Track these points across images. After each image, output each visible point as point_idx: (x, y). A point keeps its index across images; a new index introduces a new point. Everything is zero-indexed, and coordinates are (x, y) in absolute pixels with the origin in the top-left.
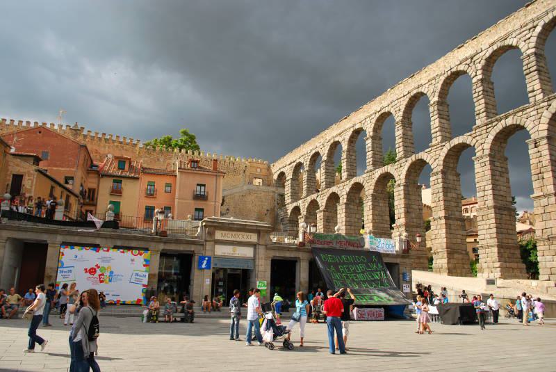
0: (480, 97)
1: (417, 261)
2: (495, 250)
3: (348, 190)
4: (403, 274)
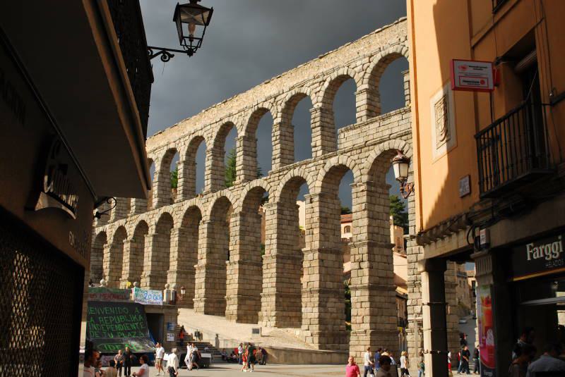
0: (277, 142)
1: (217, 305)
2: (274, 299)
3: (157, 220)
4: (168, 324)
